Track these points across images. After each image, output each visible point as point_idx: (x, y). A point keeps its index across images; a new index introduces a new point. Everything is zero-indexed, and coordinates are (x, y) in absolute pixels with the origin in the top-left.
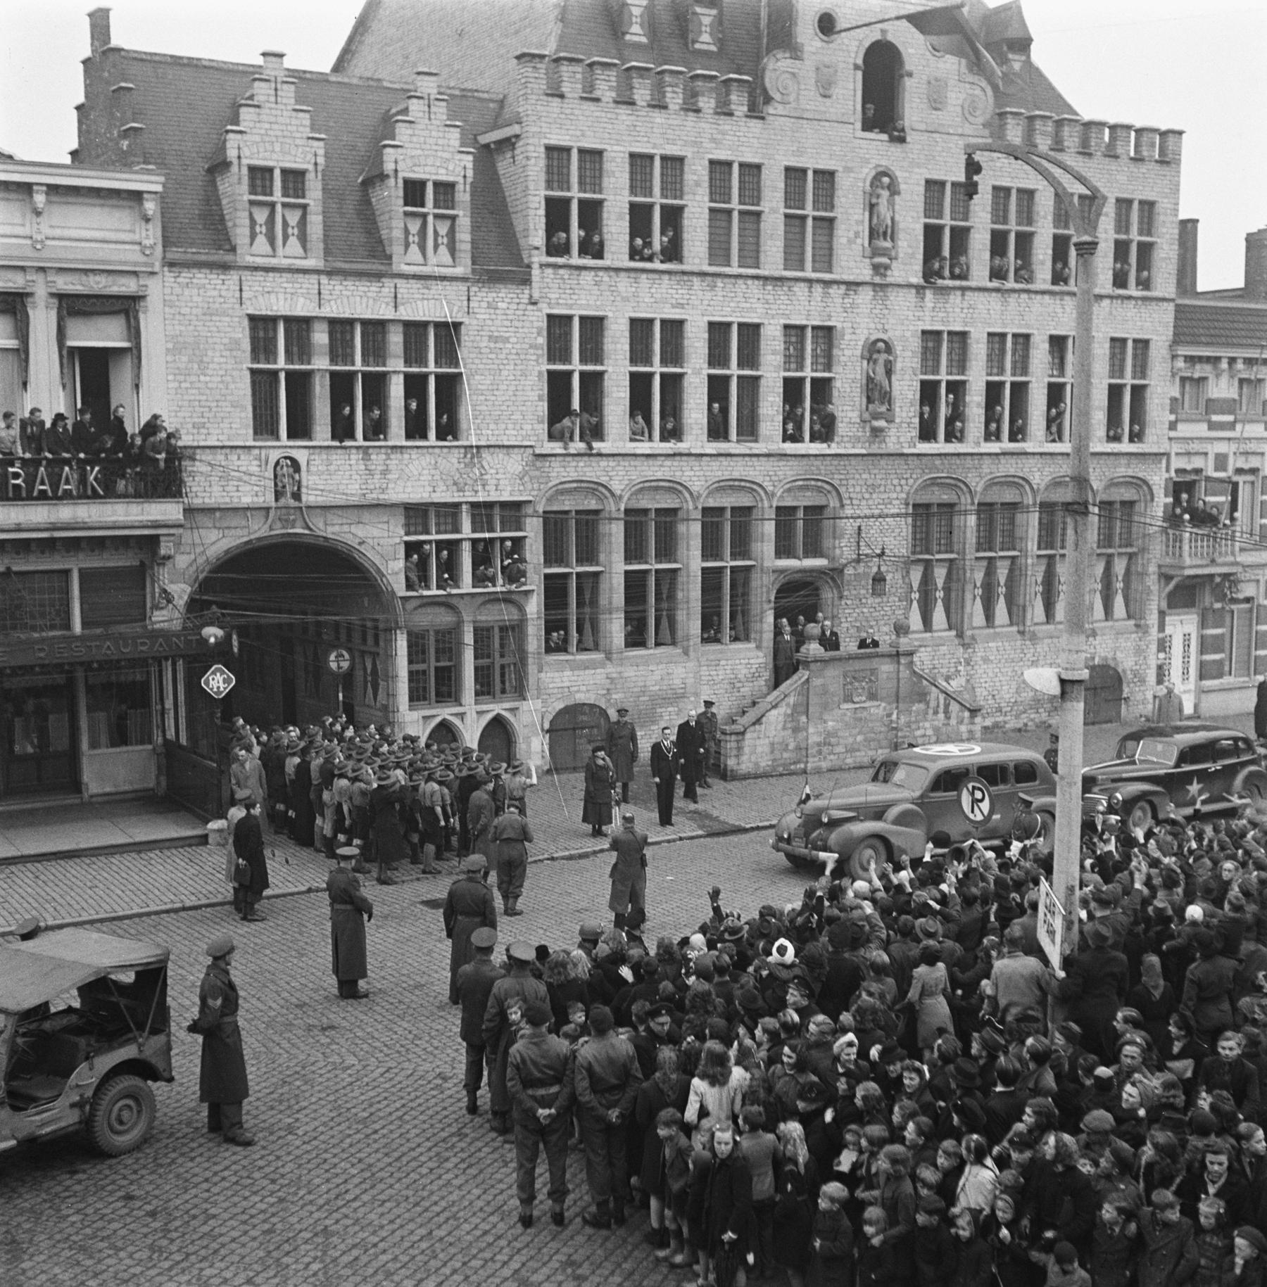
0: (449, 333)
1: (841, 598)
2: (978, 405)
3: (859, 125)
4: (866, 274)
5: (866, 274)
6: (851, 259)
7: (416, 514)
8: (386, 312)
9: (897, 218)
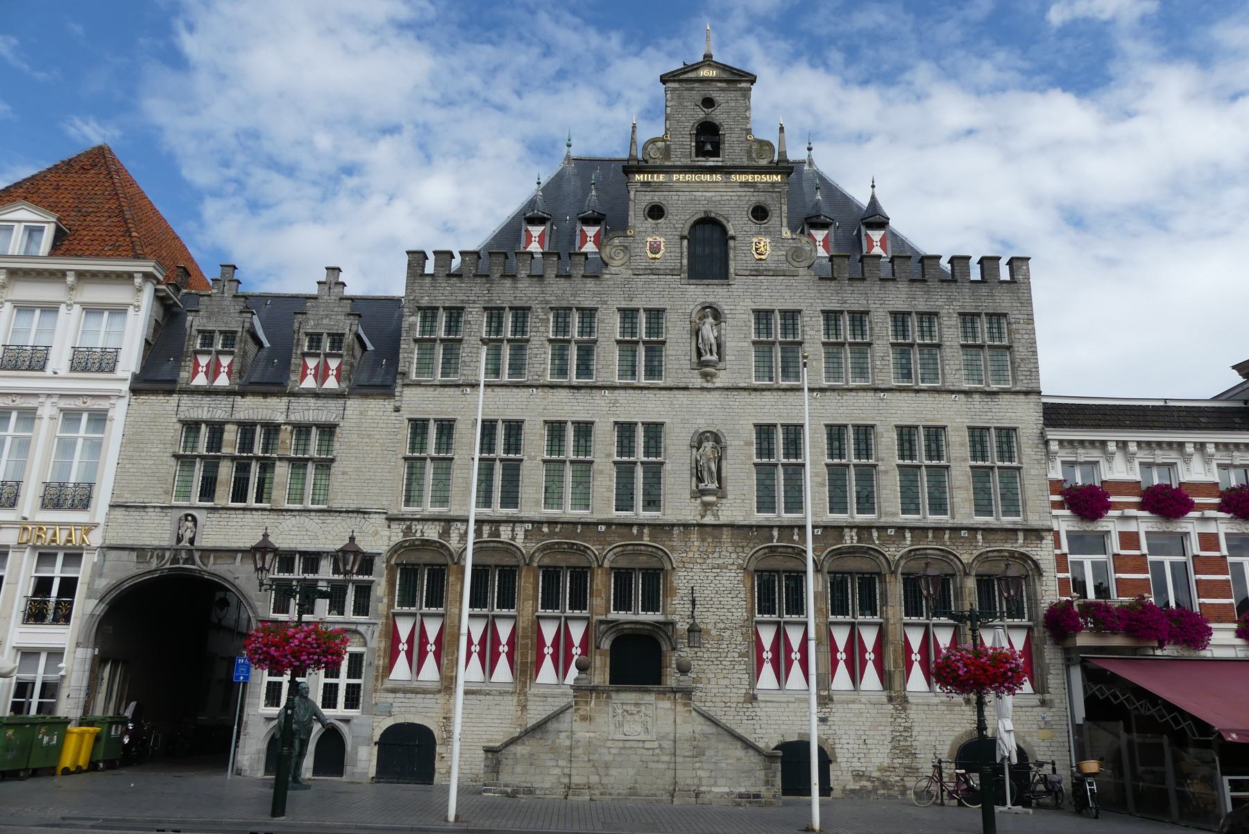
0: (328, 430)
1: (674, 649)
8: (281, 419)
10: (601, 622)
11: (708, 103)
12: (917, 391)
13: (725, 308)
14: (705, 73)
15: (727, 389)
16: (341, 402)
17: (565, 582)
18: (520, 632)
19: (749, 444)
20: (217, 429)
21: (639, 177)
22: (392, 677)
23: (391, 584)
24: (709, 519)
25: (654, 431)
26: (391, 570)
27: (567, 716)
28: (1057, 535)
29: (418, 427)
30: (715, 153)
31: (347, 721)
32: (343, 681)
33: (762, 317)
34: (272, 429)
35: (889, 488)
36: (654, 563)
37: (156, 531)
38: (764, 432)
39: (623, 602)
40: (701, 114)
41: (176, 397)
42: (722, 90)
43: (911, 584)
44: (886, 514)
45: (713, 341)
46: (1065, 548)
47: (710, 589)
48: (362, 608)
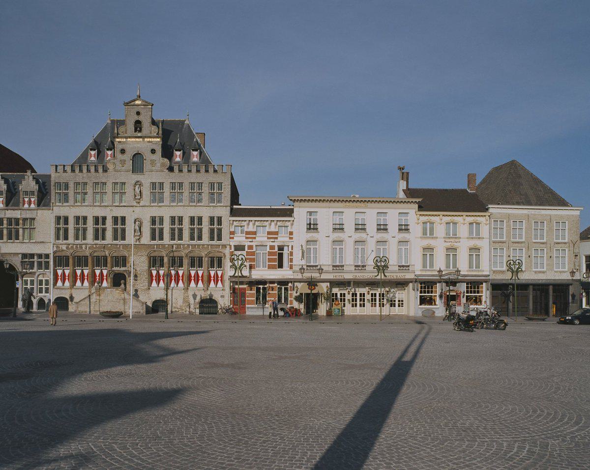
7: (24, 256)
8: (19, 217)
11: (138, 113)
14: (138, 102)
15: (143, 206)
16: (36, 211)
17: (100, 261)
19: (148, 222)
21: (117, 140)
22: (57, 285)
24: (138, 243)
25: (123, 219)
27: (95, 295)
28: (230, 246)
29: (58, 218)
30: (140, 131)
32: (44, 286)
34: (17, 221)
40: (136, 118)
42: (142, 108)
46: (233, 249)
48: (47, 267)
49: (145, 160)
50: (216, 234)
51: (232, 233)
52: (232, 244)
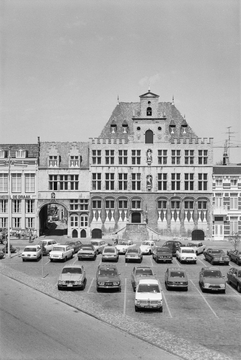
0: (77, 176)
2: (170, 185)
3: (145, 143)
4: (147, 165)
5: (147, 165)
6: (143, 162)
7: (72, 201)
9: (152, 156)
10: (130, 211)
11: (149, 102)
12: (189, 167)
13: (152, 149)
17: (123, 203)
18: (115, 213)
20: (56, 176)
23: (91, 204)
26: (91, 201)
29: (94, 175)
30: (151, 115)
31: (86, 229)
33: (160, 151)
35: (182, 185)
36: (139, 200)
37: (48, 196)
38: (160, 175)
39: (134, 207)
40: (148, 106)
41: (47, 170)
43: (186, 203)
44: (182, 190)
45: (150, 157)
47: (149, 205)
49: (154, 134)
50: (203, 185)
51: (214, 185)
52: (214, 192)
